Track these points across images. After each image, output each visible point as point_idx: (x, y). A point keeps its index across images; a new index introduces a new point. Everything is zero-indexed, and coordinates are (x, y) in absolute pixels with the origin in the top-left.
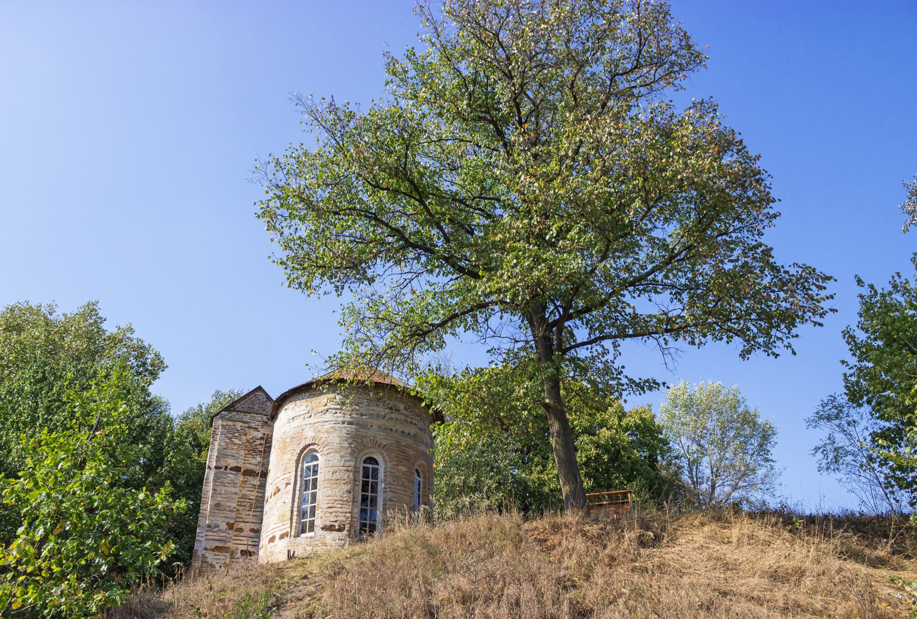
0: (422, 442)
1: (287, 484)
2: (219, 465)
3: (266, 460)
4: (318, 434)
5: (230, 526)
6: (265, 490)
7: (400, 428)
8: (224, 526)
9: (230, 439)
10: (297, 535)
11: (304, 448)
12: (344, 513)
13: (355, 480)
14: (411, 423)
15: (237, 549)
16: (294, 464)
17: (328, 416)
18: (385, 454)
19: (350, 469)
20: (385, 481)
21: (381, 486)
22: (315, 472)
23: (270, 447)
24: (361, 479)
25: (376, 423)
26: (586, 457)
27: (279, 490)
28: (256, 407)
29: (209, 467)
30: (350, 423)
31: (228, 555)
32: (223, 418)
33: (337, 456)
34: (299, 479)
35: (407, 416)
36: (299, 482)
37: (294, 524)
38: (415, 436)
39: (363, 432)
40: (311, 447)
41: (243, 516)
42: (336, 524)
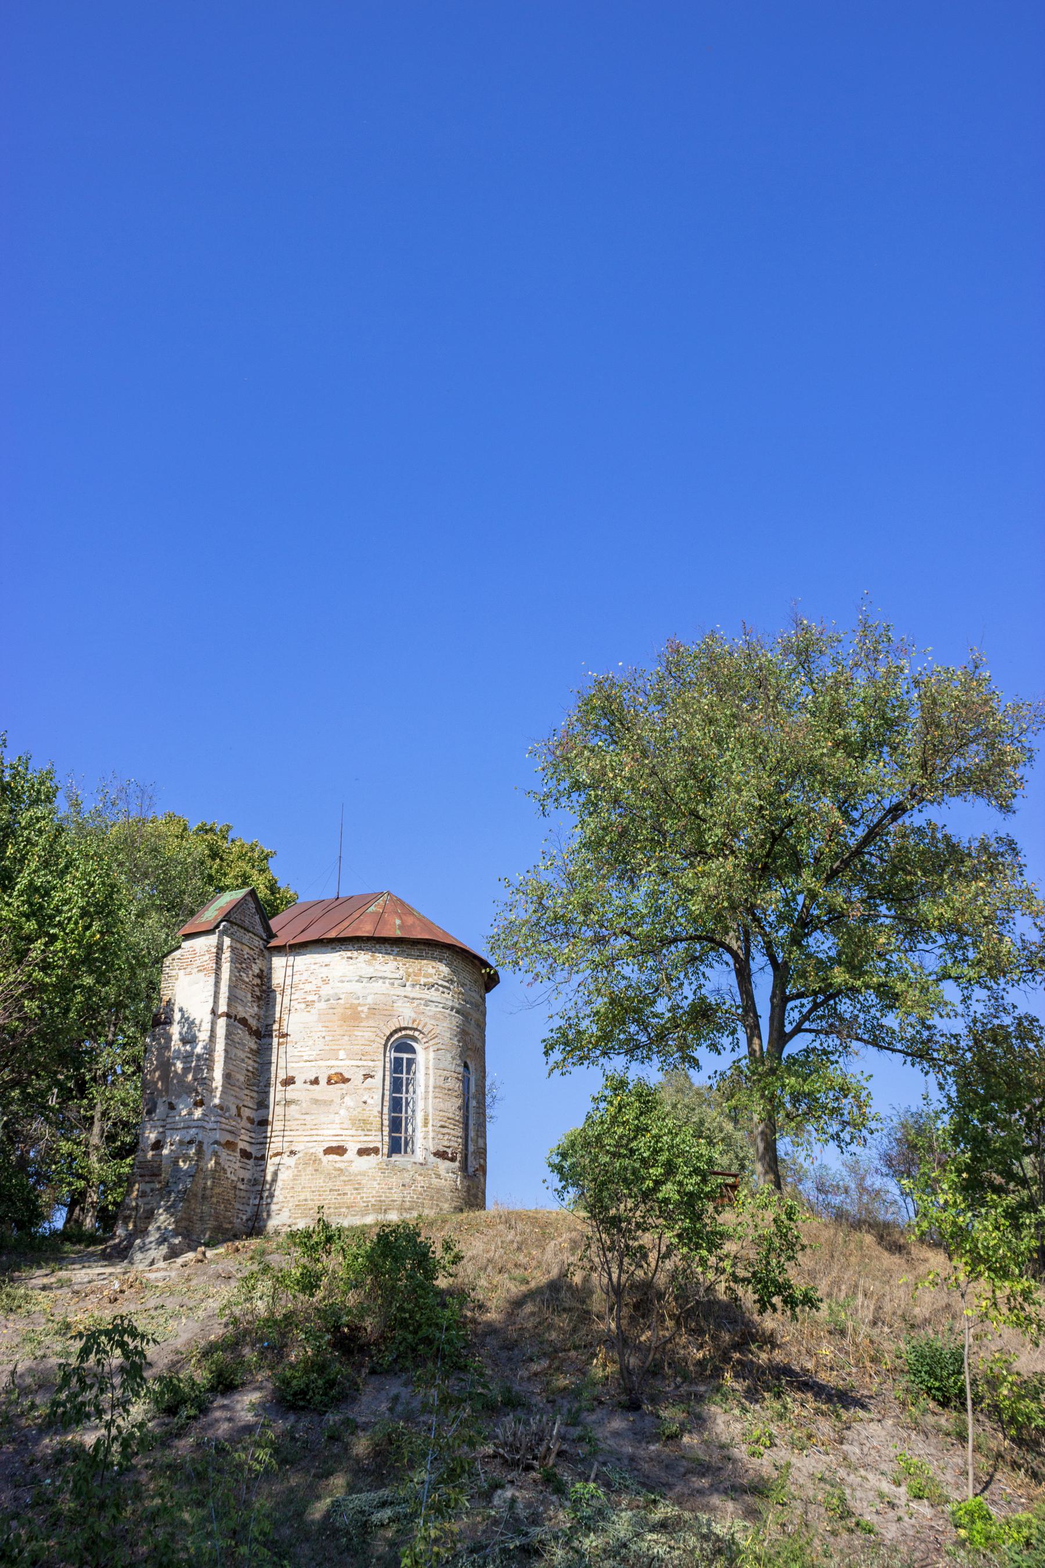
17: (433, 994)
33: (449, 1056)
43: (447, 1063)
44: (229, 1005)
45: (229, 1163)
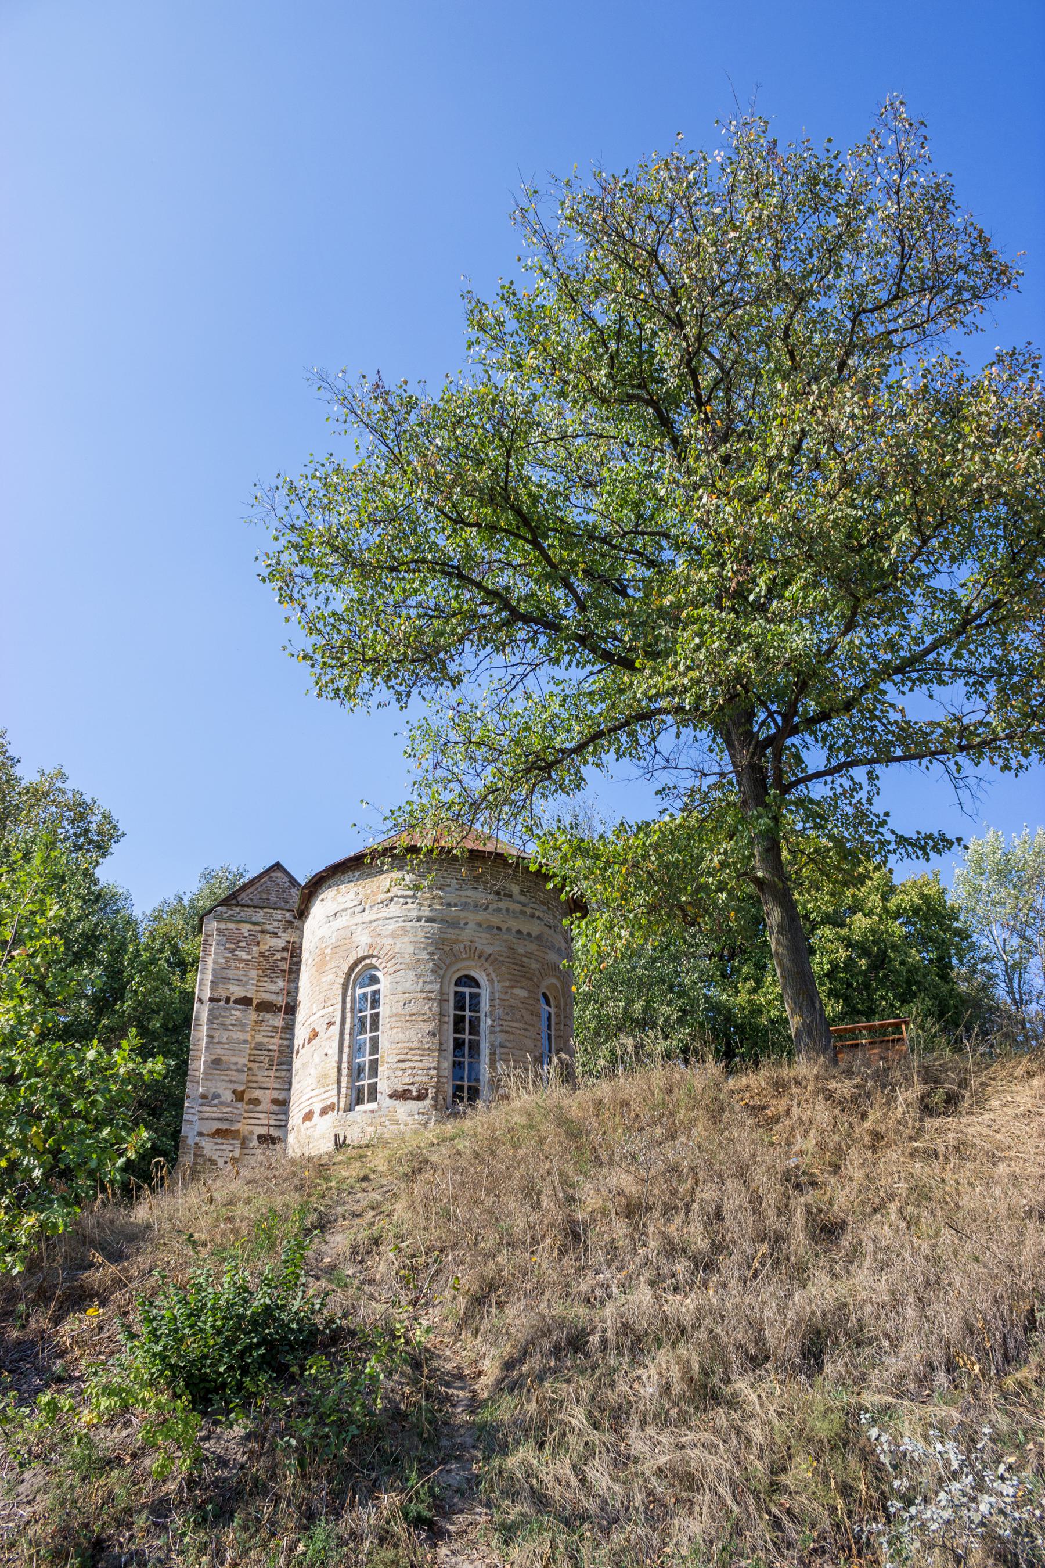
0: (552, 947)
1: (330, 1024)
2: (216, 995)
3: (292, 985)
4: (378, 940)
5: (239, 1096)
6: (293, 1035)
7: (514, 925)
8: (228, 1096)
9: (232, 951)
10: (349, 1109)
11: (356, 964)
12: (426, 1069)
13: (442, 1014)
14: (533, 916)
15: (251, 1133)
16: (340, 991)
17: (394, 909)
18: (491, 970)
19: (433, 995)
20: (492, 1014)
21: (486, 1023)
22: (375, 1003)
23: (298, 963)
24: (452, 1012)
25: (473, 918)
26: (830, 963)
27: (316, 1035)
28: (273, 898)
29: (200, 1000)
30: (429, 920)
31: (237, 1143)
32: (219, 918)
33: (411, 975)
34: (348, 1015)
35: (524, 905)
36: (348, 1021)
37: (344, 1090)
38: (539, 938)
39: (452, 934)
40: (368, 961)
41: (259, 1078)
42: (414, 1089)
43: (408, 985)
44: (212, 989)
45: (218, 1153)
